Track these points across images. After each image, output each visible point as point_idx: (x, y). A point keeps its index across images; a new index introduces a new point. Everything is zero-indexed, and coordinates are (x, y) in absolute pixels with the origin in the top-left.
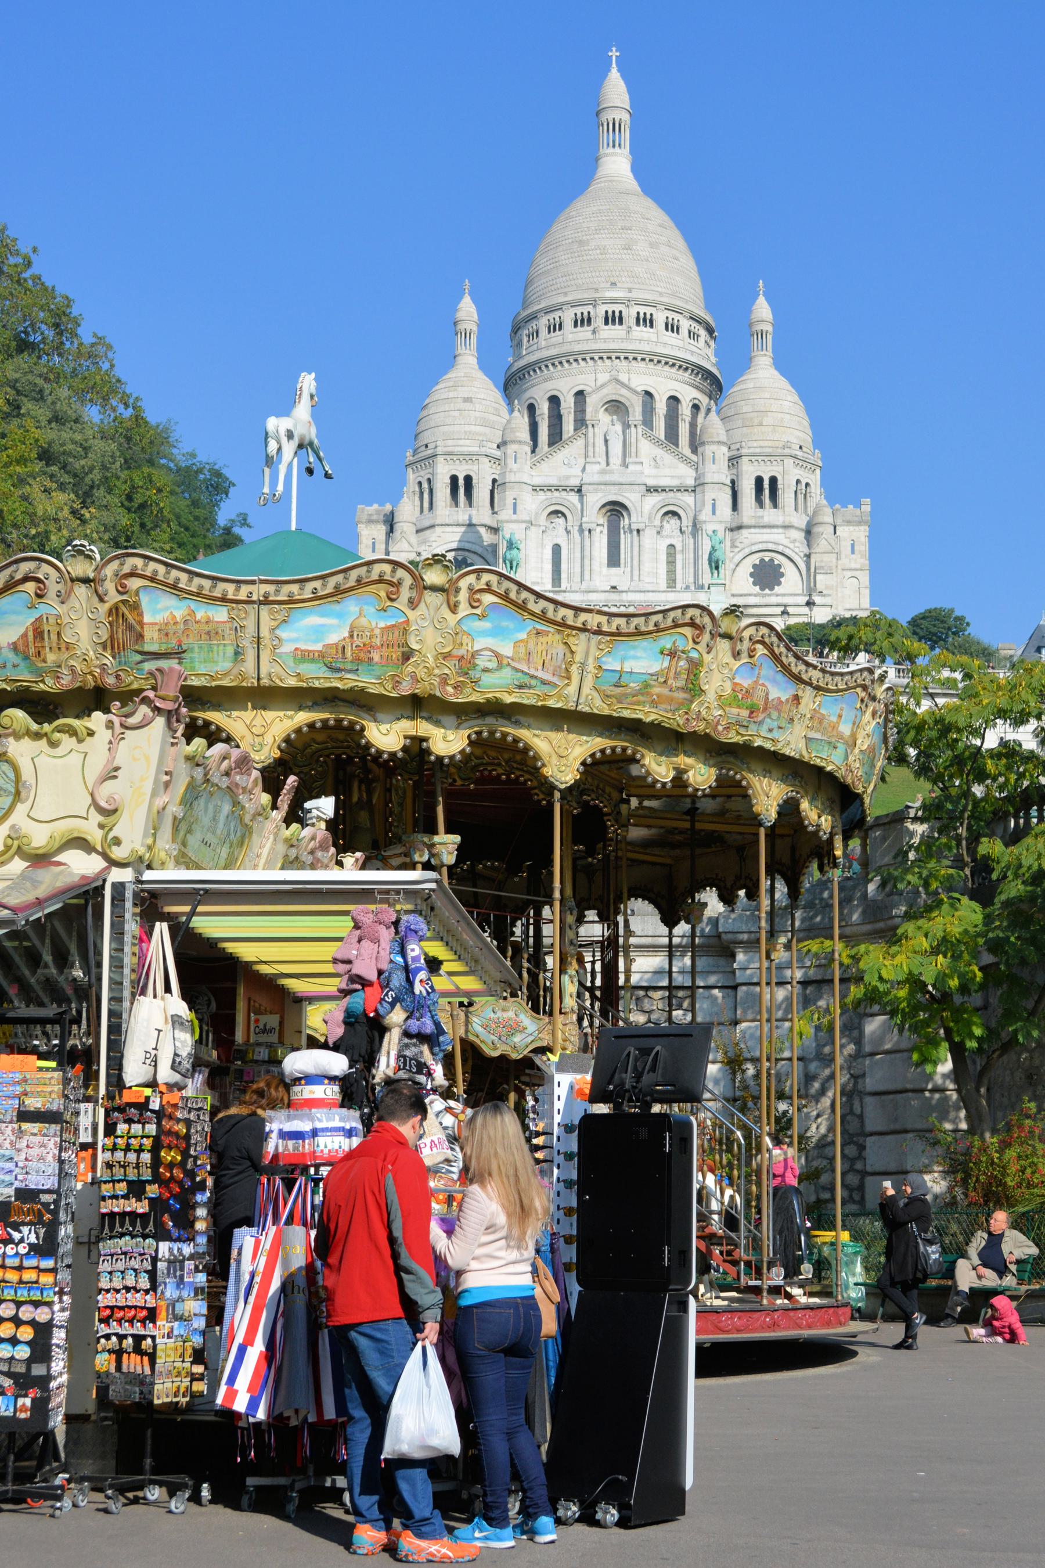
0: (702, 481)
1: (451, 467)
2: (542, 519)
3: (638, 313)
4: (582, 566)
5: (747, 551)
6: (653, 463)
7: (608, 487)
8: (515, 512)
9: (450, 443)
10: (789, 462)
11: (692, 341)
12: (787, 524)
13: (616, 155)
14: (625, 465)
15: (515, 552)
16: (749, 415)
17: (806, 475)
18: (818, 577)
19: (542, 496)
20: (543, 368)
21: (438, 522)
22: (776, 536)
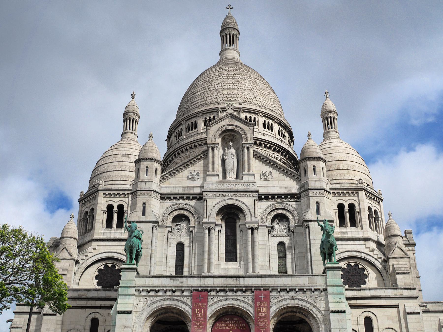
0: (306, 187)
2: (169, 222)
3: (246, 117)
4: (203, 260)
6: (262, 177)
7: (225, 194)
8: (144, 214)
9: (110, 183)
10: (362, 194)
11: (281, 137)
12: (366, 236)
17: (374, 204)
18: (398, 276)
19: (168, 203)
20: (184, 150)
21: (95, 237)
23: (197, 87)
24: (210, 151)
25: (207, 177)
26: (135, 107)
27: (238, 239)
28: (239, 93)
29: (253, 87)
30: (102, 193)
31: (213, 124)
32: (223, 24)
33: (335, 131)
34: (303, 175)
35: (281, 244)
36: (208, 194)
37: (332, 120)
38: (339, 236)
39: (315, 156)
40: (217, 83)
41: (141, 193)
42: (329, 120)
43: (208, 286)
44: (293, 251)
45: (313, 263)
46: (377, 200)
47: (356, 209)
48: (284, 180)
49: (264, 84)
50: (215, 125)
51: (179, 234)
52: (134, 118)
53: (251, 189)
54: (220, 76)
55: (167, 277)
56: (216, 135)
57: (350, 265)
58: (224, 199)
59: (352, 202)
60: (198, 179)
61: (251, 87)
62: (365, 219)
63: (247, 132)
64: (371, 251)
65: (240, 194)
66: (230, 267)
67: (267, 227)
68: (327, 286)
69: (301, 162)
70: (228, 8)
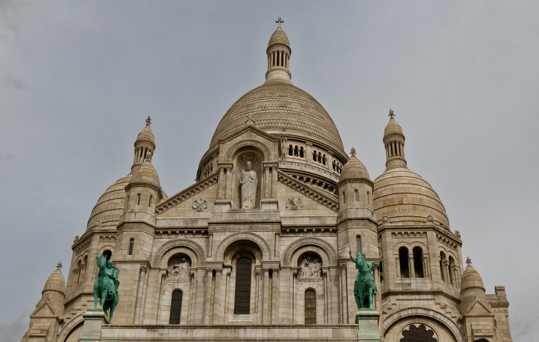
0: (344, 217)
1: (106, 244)
2: (164, 264)
3: (291, 146)
5: (396, 317)
7: (237, 226)
8: (130, 253)
9: (109, 224)
10: (432, 234)
11: (336, 172)
12: (435, 289)
13: (280, 69)
14: (257, 206)
15: (106, 281)
16: (389, 197)
17: (448, 249)
19: (165, 239)
22: (425, 302)
23: (233, 113)
24: (222, 173)
25: (216, 206)
26: (149, 134)
27: (253, 284)
28: (283, 118)
29: (302, 111)
30: (98, 237)
31: (228, 140)
32: (271, 40)
33: (400, 159)
34: (342, 202)
35: (310, 291)
36: (215, 226)
37: (397, 145)
38: (399, 288)
39: (358, 176)
40: (256, 107)
41: (129, 225)
42: (393, 145)
43: (196, 339)
44: (326, 299)
45: (349, 315)
46: (452, 244)
47: (423, 254)
48: (317, 209)
49: (316, 108)
50: (230, 141)
51: (177, 279)
52: (147, 148)
53: (271, 220)
54: (261, 99)
55: (143, 327)
56: (229, 154)
57: (414, 326)
58: (237, 232)
59: (418, 245)
60: (205, 208)
61: (299, 111)
62: (435, 267)
63: (270, 149)
64: (442, 308)
65: (256, 226)
66: (240, 321)
67: (291, 268)
68: (358, 340)
69: (339, 186)
70: (278, 22)
